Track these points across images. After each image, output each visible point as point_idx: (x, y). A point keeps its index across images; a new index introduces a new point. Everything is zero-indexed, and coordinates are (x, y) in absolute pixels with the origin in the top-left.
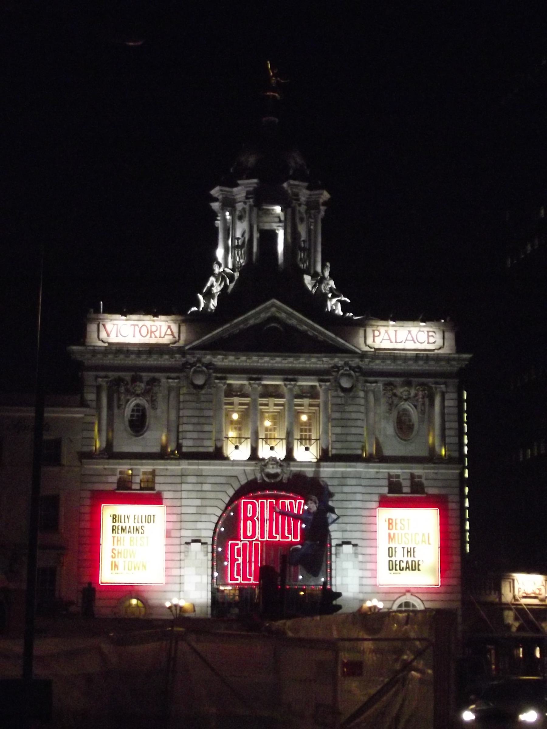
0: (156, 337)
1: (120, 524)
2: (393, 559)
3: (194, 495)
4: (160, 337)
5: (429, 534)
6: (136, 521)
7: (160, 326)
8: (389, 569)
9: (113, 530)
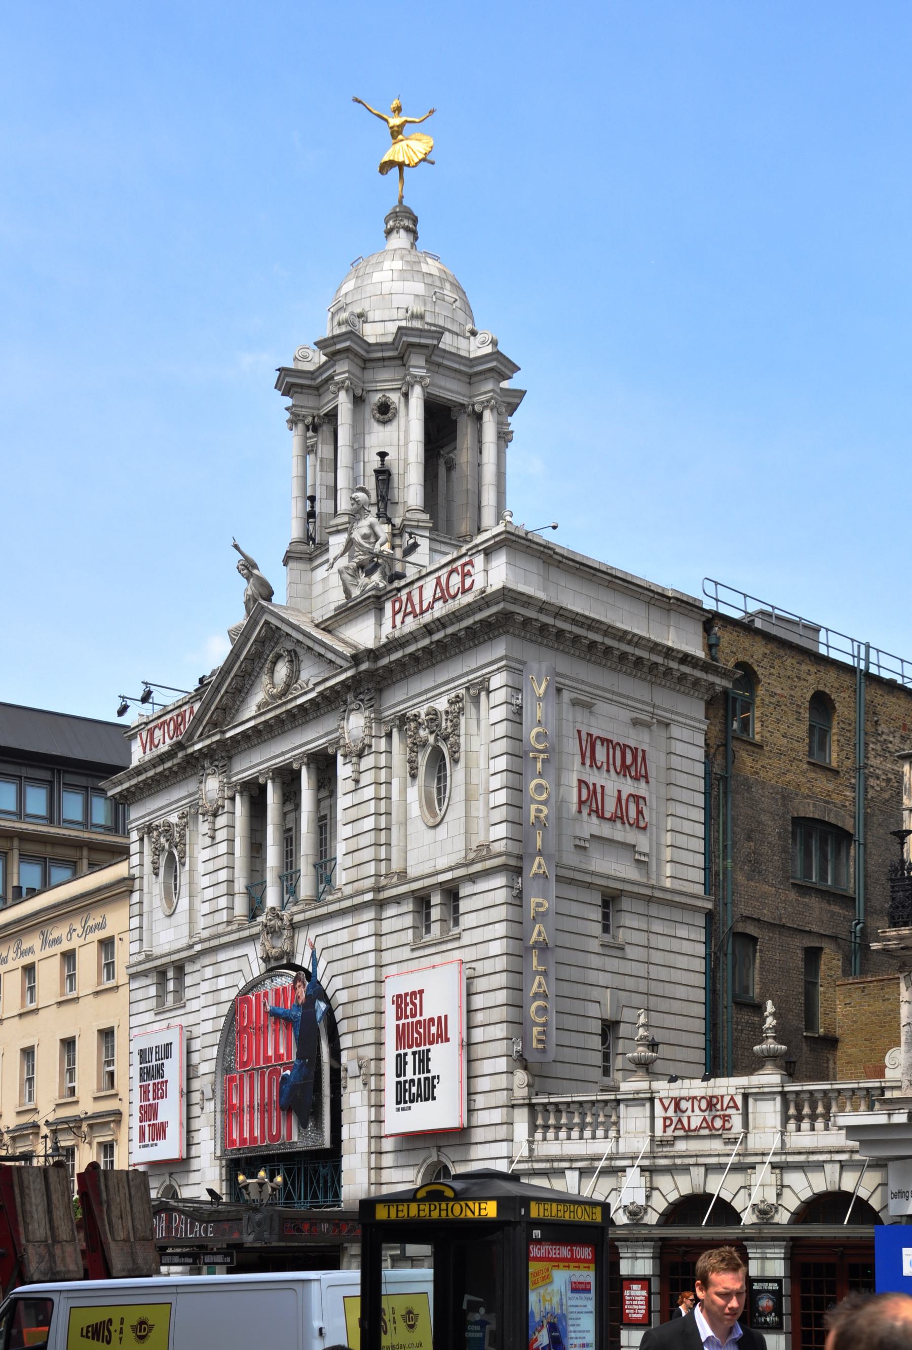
1: (145, 1065)
2: (402, 1079)
5: (446, 1017)
8: (398, 1103)
9: (141, 1075)
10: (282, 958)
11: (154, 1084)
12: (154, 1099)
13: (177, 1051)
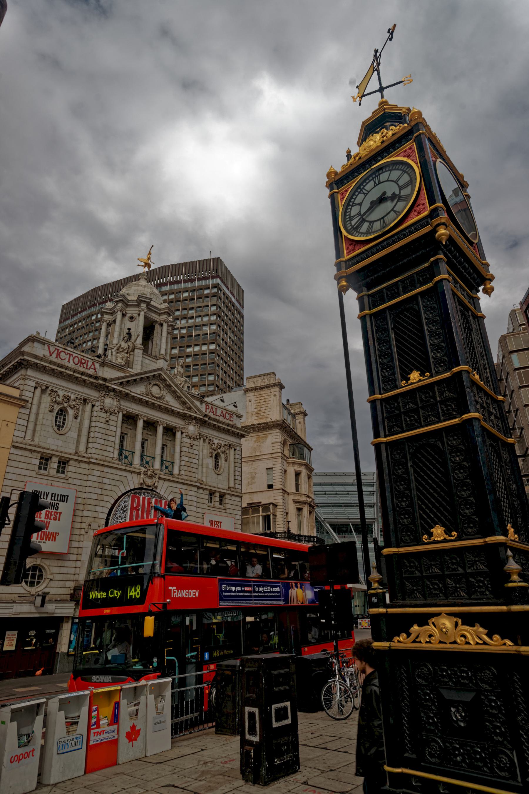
0: (83, 367)
3: (96, 485)
4: (87, 368)
6: (53, 498)
7: (88, 361)
10: (150, 487)
11: (47, 511)
12: (45, 518)
13: (71, 500)
